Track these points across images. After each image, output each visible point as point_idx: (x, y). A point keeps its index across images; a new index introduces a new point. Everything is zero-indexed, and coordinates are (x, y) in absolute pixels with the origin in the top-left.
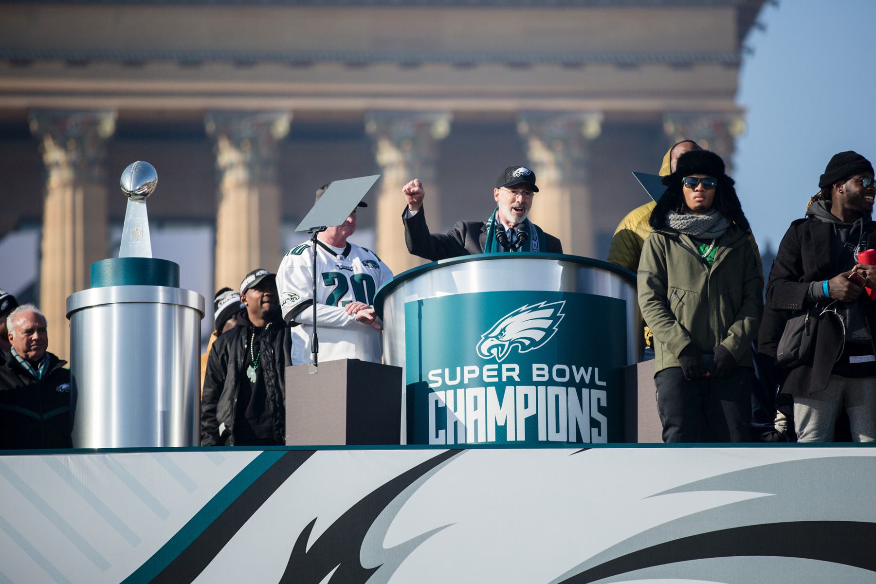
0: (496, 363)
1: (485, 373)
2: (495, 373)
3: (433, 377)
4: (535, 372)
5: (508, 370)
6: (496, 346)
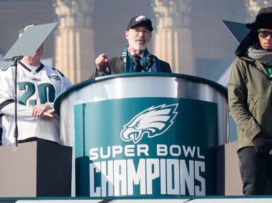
0: (133, 144)
1: (126, 151)
3: (93, 153)
4: (159, 150)
5: (141, 148)
6: (134, 133)
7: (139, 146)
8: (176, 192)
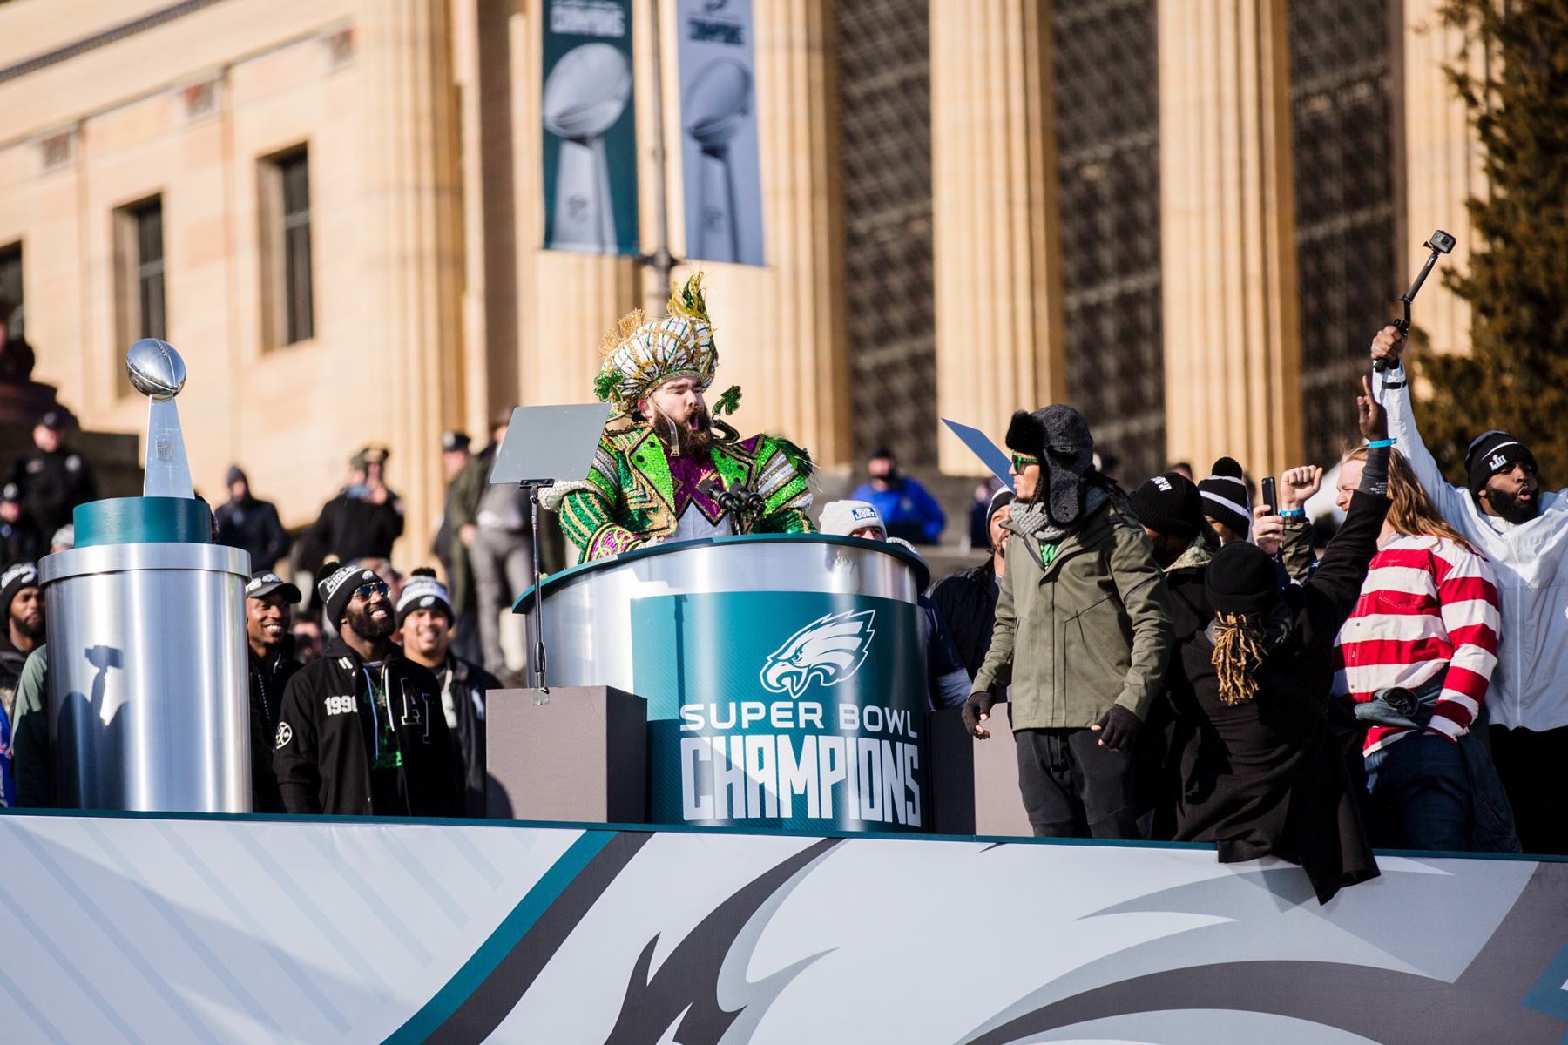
1: (775, 715)
2: (789, 715)
5: (808, 711)
6: (789, 674)
7: (802, 706)
8: (875, 815)
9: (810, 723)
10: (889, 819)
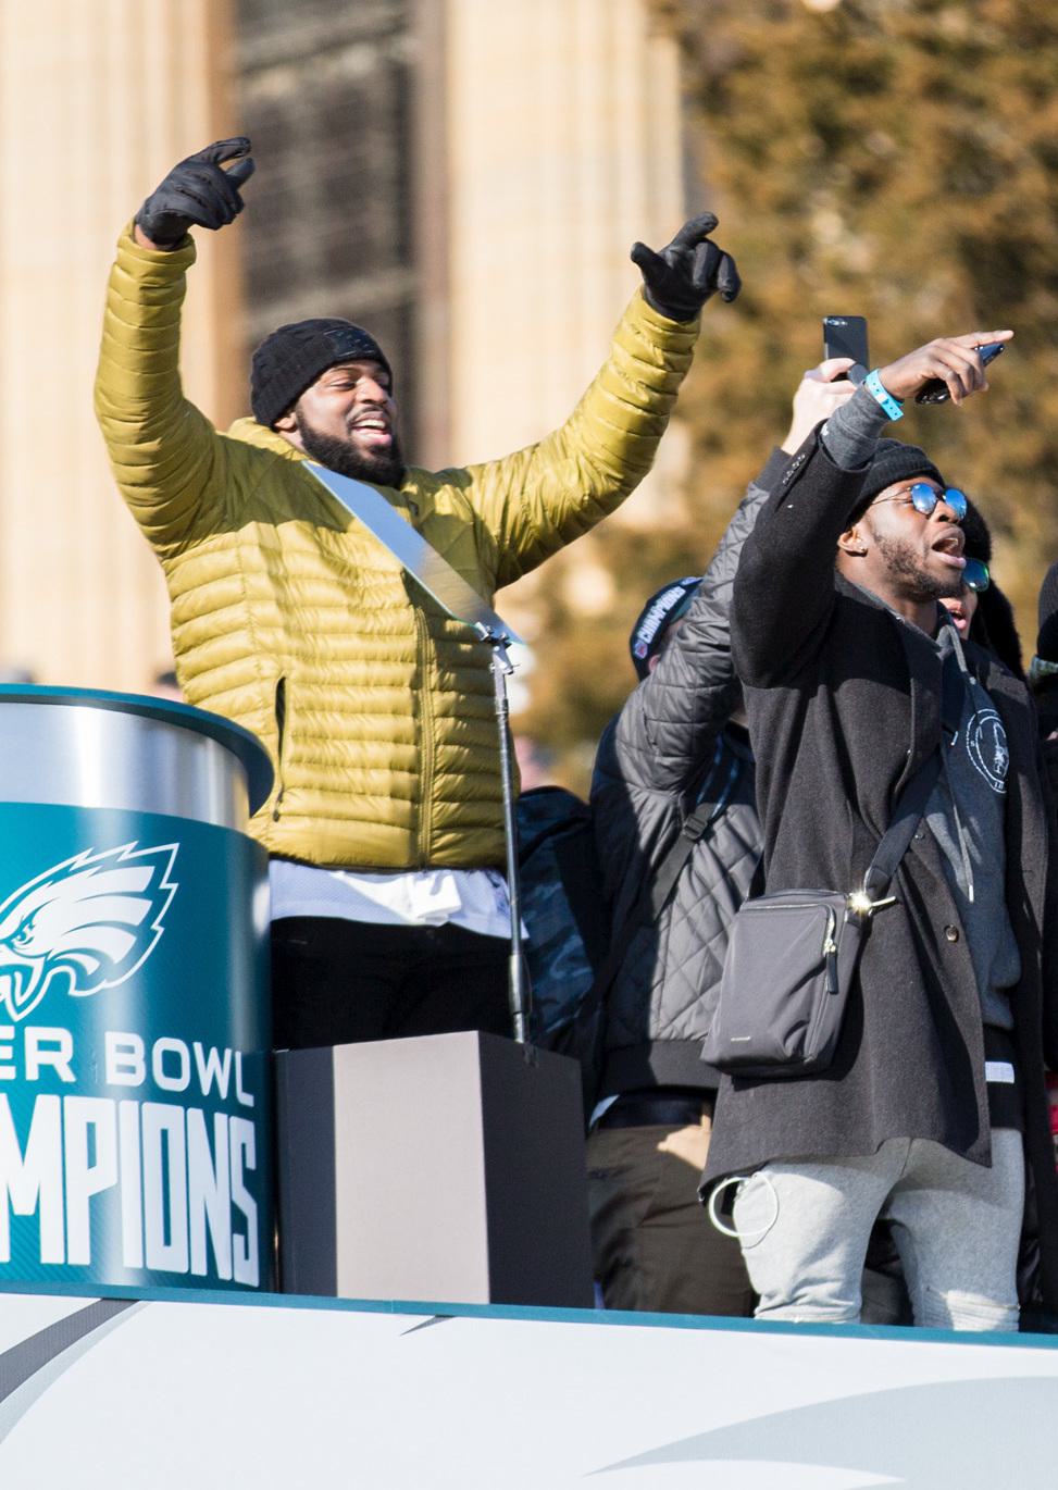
5: (45, 1046)
9: (47, 1071)
10: (200, 1269)
